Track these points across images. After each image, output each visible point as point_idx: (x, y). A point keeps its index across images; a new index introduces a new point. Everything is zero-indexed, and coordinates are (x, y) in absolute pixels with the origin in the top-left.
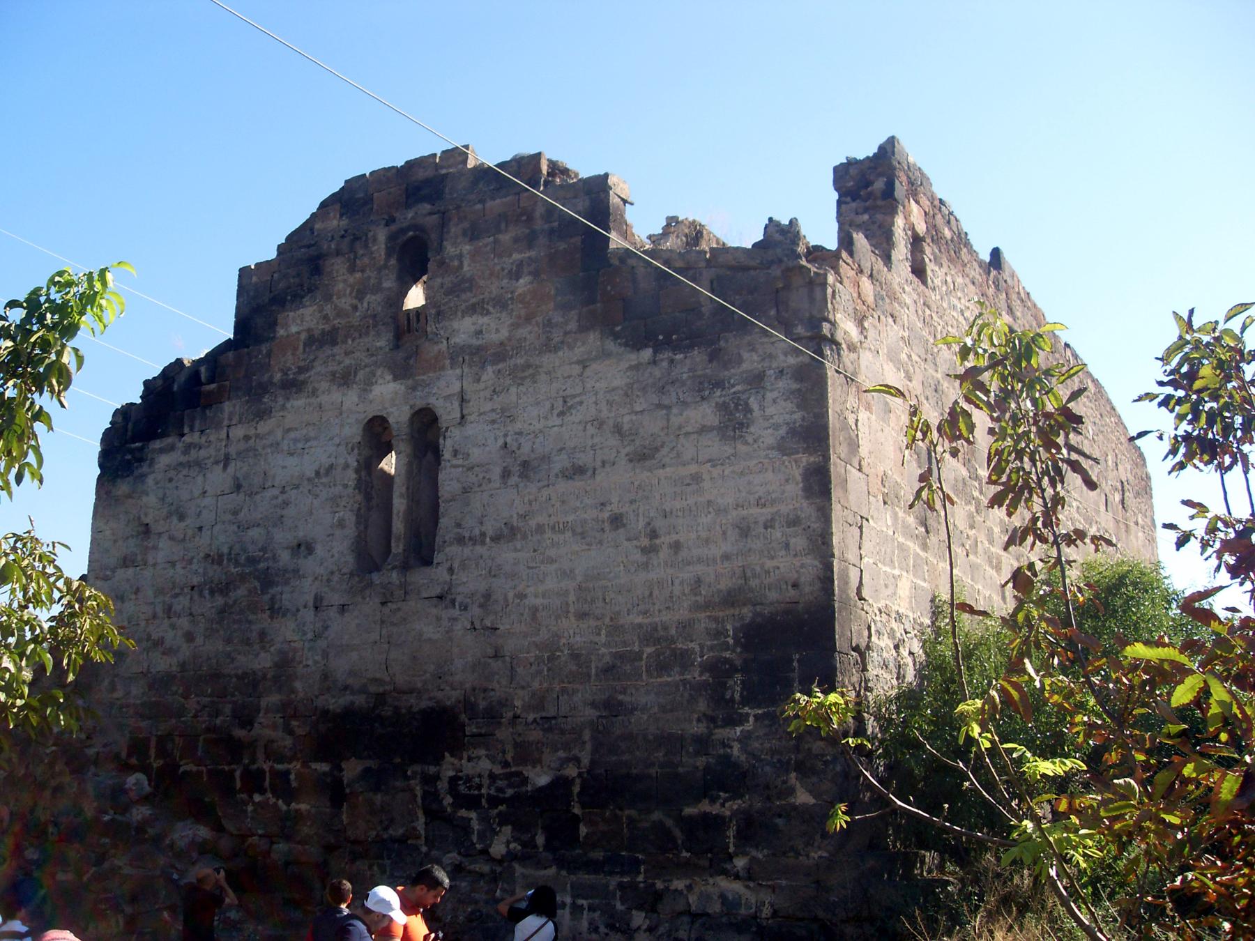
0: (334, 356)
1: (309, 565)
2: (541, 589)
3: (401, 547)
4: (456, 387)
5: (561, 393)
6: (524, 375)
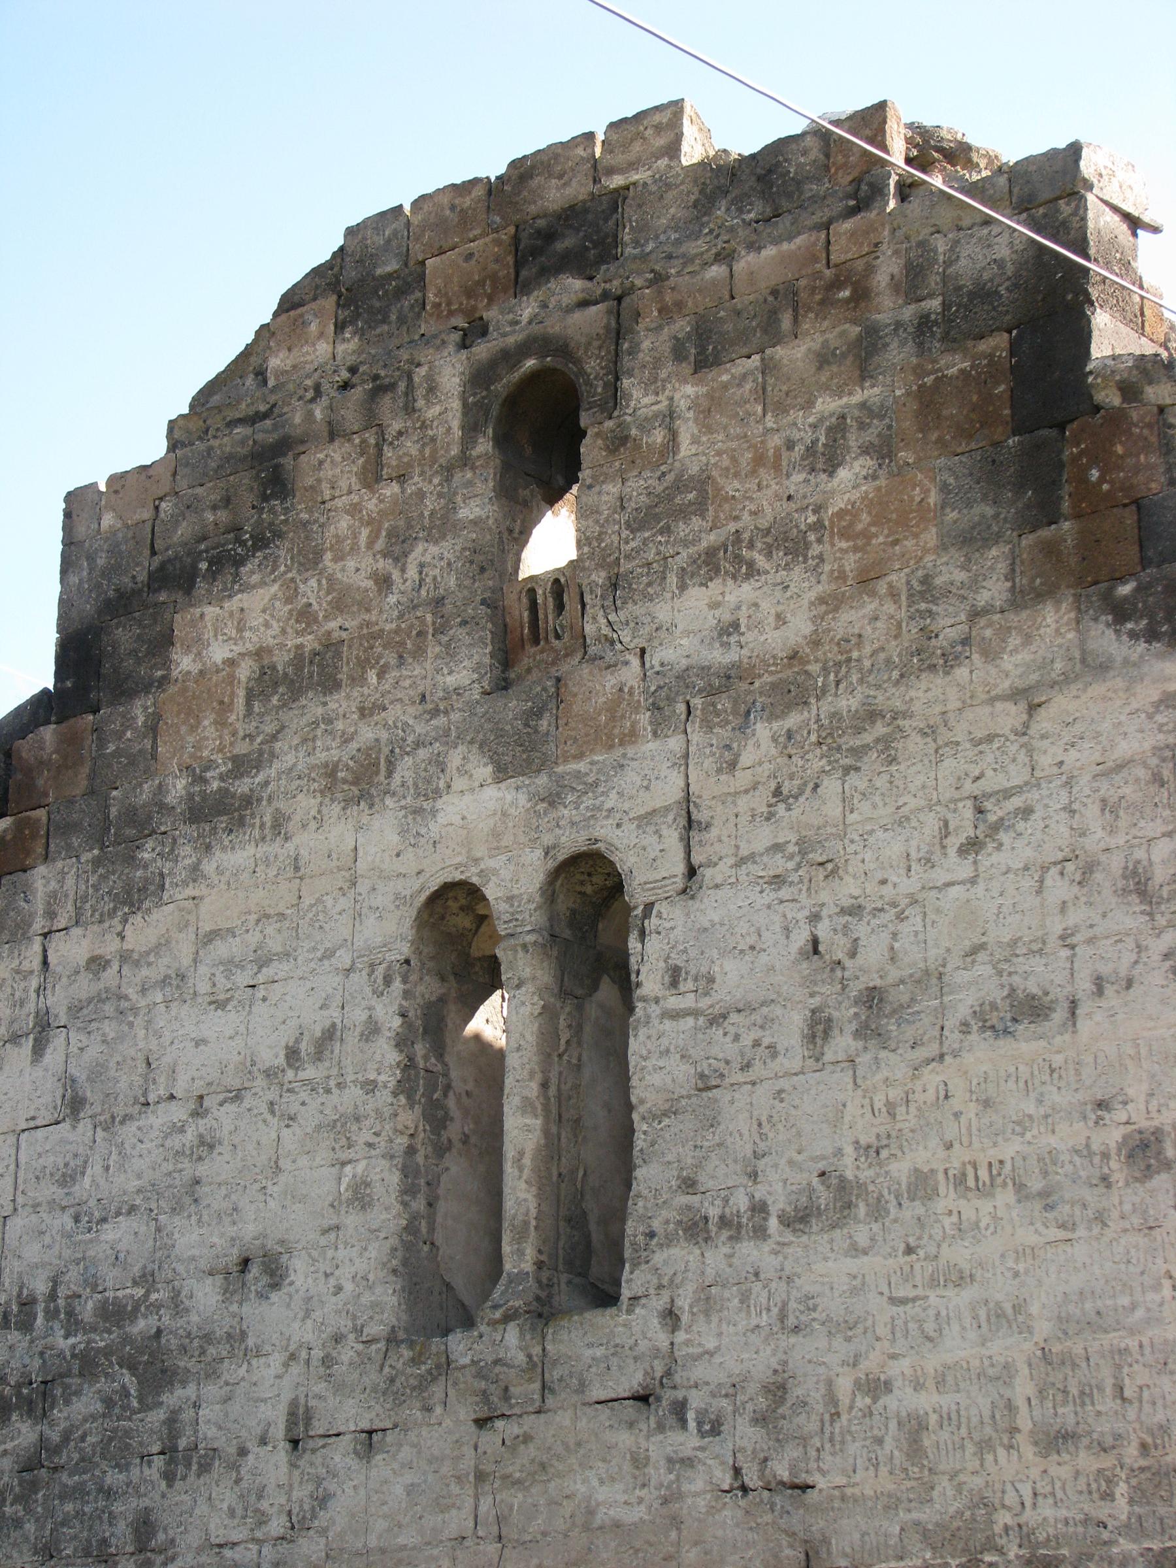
0: (329, 721)
1: (273, 1318)
2: (932, 1362)
3: (530, 1253)
4: (669, 790)
5: (969, 787)
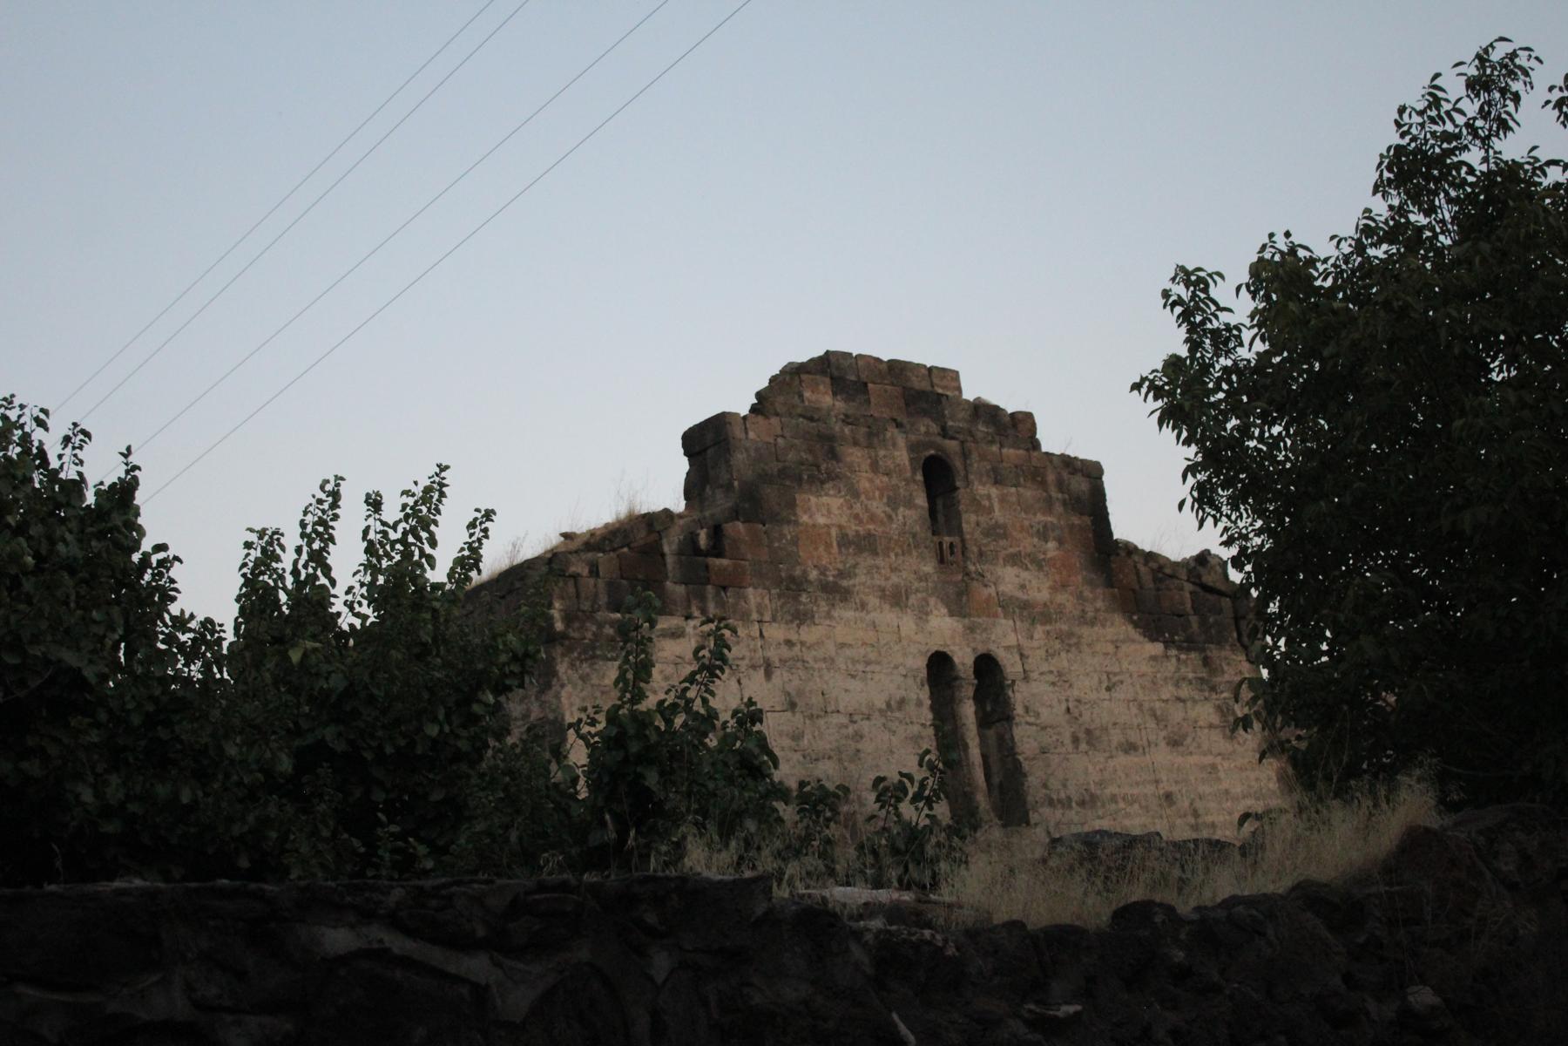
6: (1068, 641)
